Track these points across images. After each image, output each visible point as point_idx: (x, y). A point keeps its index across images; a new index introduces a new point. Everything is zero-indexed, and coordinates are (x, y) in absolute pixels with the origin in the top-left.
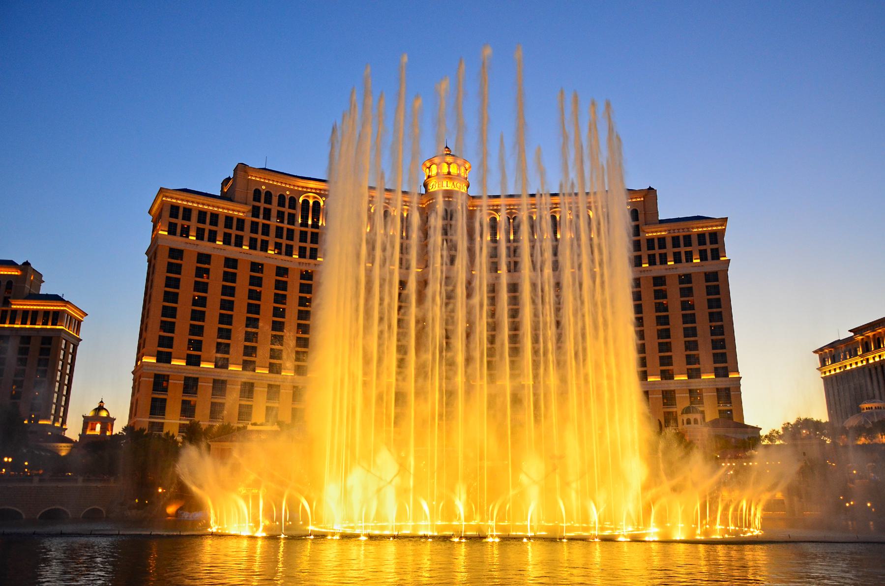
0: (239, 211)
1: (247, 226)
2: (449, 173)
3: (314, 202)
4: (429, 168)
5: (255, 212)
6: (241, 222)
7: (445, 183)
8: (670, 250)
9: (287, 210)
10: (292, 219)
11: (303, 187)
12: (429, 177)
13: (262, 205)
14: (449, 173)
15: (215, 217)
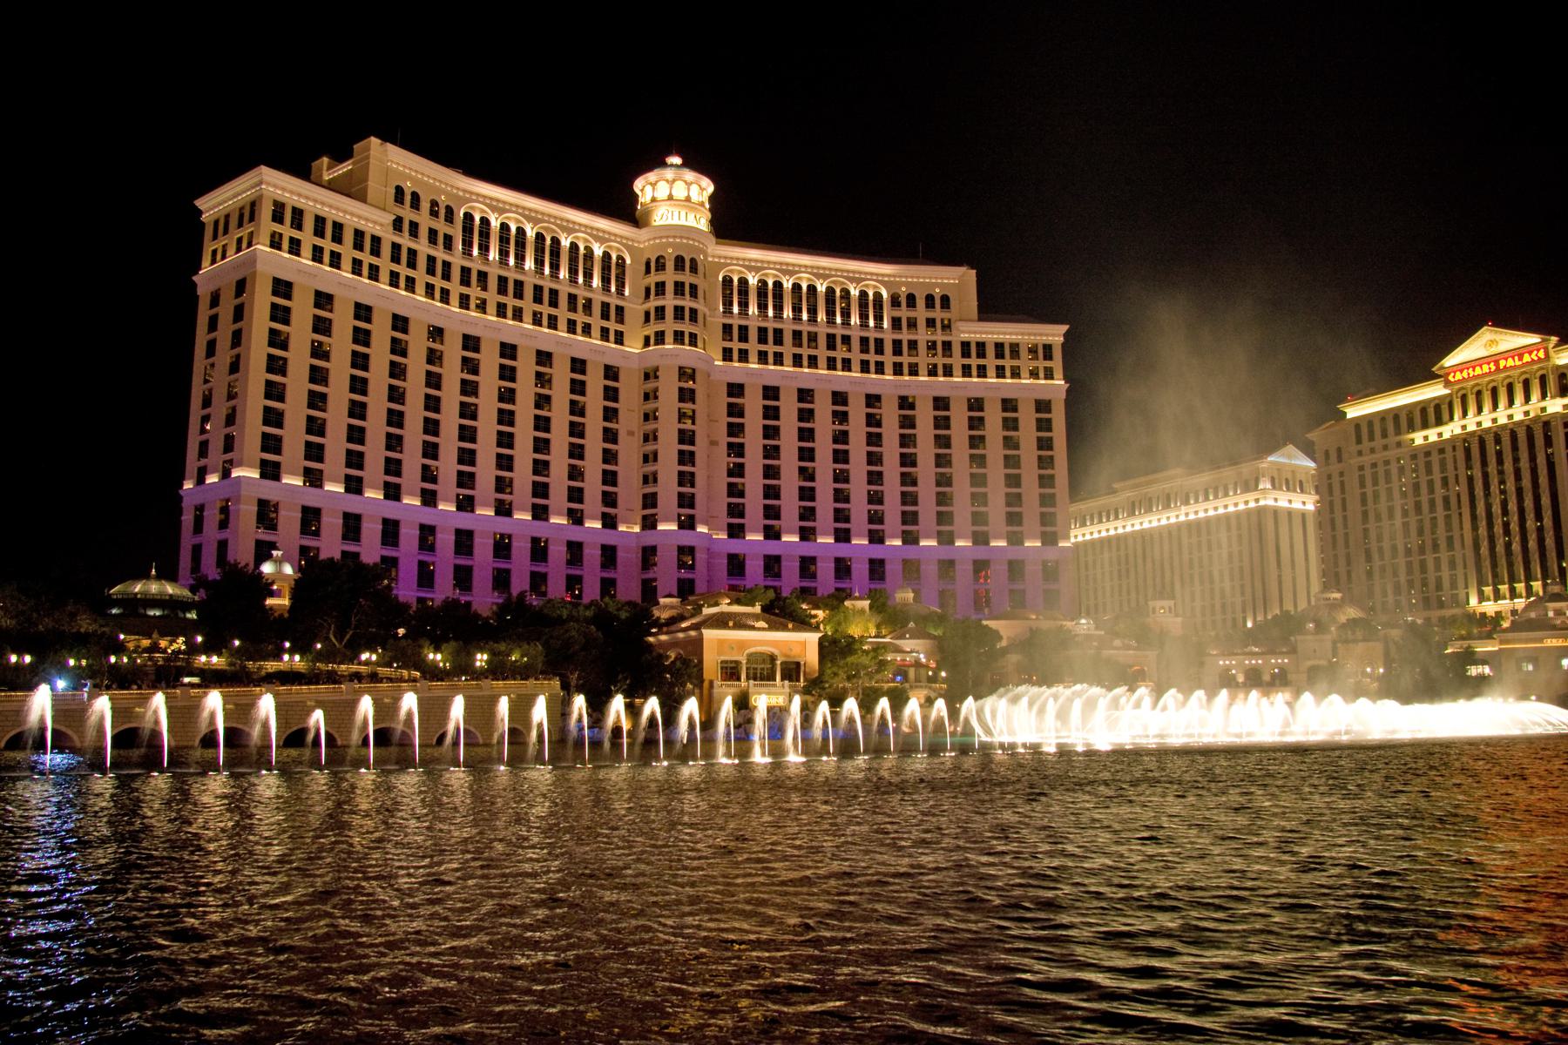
0: (375, 223)
1: (386, 250)
2: (688, 199)
3: (482, 219)
4: (654, 185)
5: (398, 224)
6: (376, 241)
7: (683, 214)
8: (991, 361)
9: (442, 227)
10: (448, 242)
11: (465, 191)
12: (654, 200)
13: (408, 214)
14: (688, 199)
15: (338, 227)
